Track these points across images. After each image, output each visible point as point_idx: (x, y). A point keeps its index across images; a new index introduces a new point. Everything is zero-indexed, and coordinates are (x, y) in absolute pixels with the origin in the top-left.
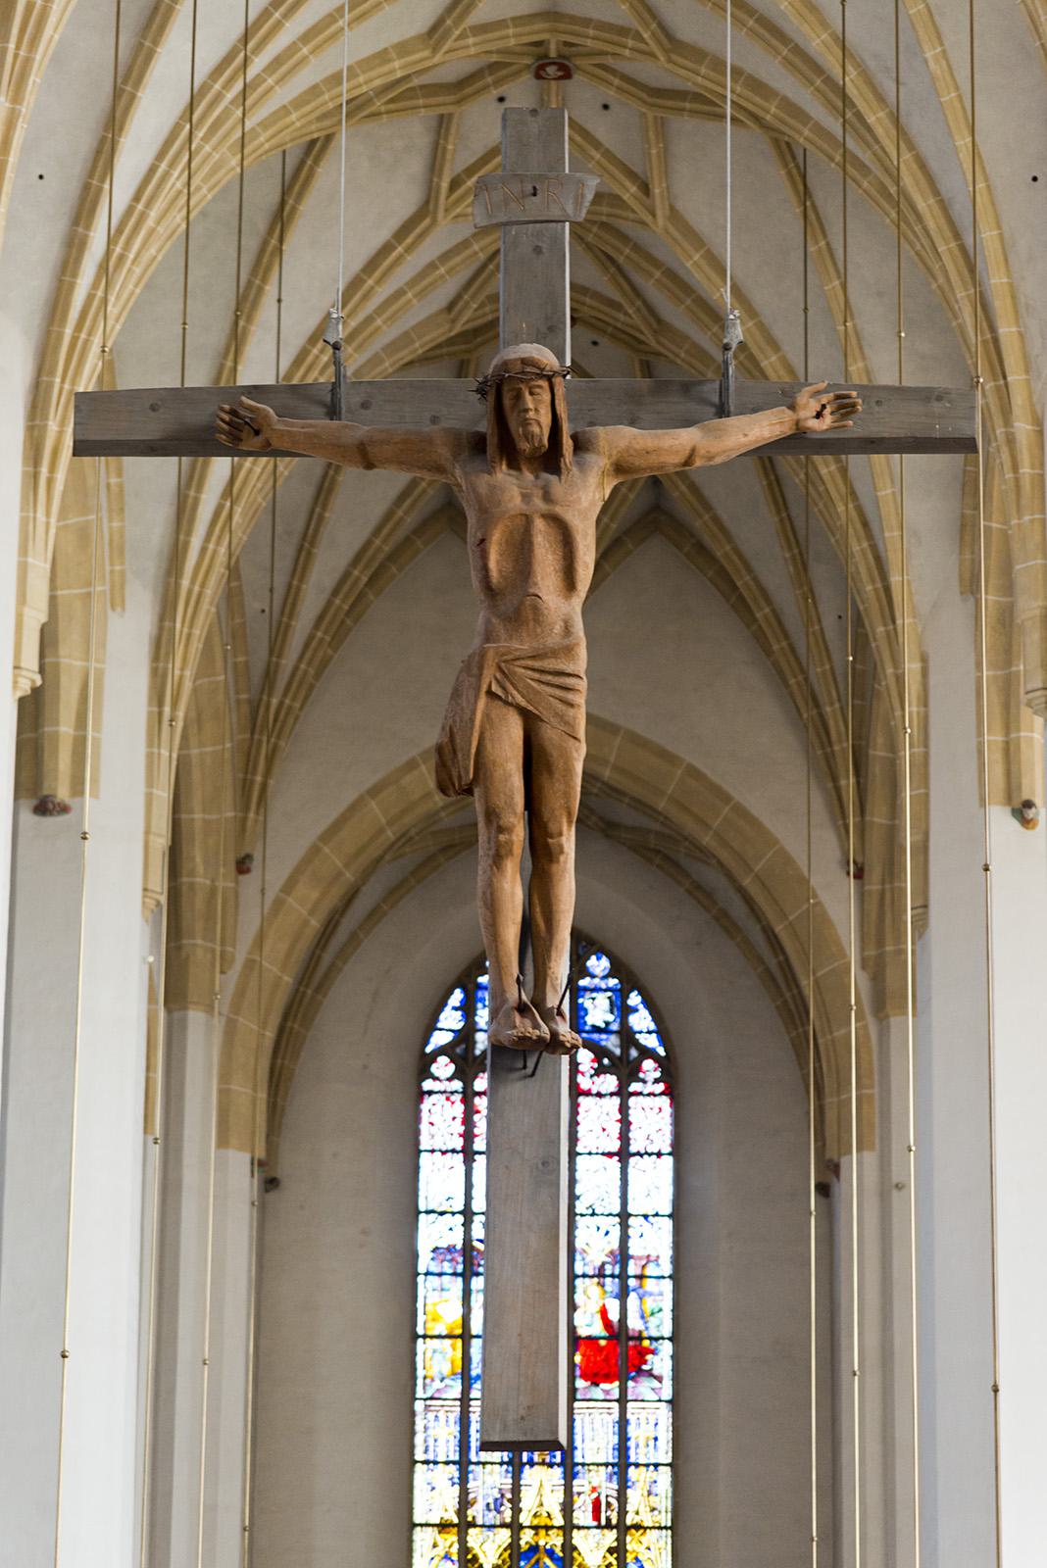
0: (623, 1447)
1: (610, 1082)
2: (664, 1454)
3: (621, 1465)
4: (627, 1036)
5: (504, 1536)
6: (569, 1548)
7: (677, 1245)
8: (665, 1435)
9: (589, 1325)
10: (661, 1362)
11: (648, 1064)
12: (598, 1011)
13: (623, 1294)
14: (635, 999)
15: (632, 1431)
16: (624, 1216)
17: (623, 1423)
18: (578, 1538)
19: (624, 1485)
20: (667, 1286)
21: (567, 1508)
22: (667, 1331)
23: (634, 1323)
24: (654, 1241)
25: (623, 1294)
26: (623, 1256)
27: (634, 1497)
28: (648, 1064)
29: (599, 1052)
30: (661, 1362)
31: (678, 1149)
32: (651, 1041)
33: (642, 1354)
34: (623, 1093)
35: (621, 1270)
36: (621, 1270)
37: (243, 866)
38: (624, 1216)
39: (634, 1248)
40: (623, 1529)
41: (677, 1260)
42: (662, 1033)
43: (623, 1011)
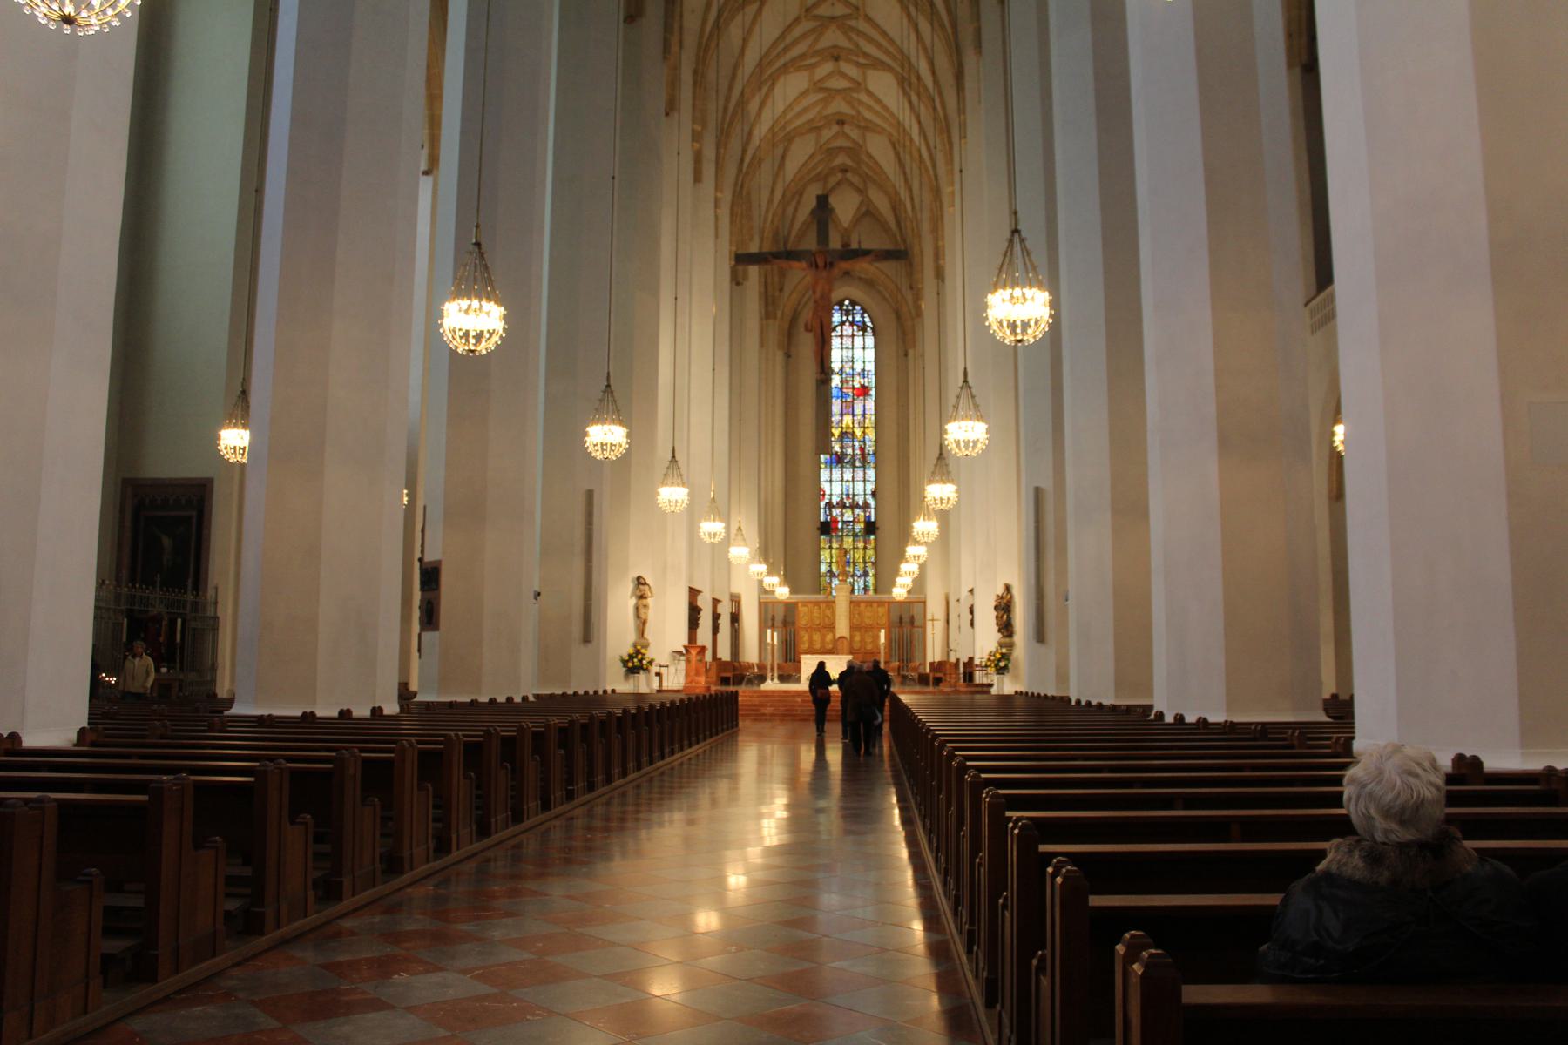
0: (864, 411)
1: (861, 333)
2: (873, 412)
3: (864, 415)
4: (864, 323)
5: (840, 429)
6: (853, 432)
7: (876, 368)
8: (873, 408)
9: (857, 385)
10: (873, 392)
11: (869, 329)
12: (858, 318)
13: (864, 378)
14: (866, 315)
15: (866, 407)
16: (864, 362)
17: (864, 406)
18: (855, 430)
19: (865, 418)
20: (874, 377)
21: (853, 423)
22: (873, 385)
23: (866, 384)
24: (871, 367)
25: (864, 378)
26: (864, 370)
27: (867, 421)
28: (869, 329)
29: (858, 326)
30: (873, 392)
31: (875, 347)
32: (869, 324)
33: (868, 391)
34: (863, 335)
35: (863, 373)
36: (863, 373)
37: (781, 290)
38: (864, 362)
39: (866, 369)
40: (865, 428)
41: (875, 371)
42: (872, 322)
43: (863, 317)
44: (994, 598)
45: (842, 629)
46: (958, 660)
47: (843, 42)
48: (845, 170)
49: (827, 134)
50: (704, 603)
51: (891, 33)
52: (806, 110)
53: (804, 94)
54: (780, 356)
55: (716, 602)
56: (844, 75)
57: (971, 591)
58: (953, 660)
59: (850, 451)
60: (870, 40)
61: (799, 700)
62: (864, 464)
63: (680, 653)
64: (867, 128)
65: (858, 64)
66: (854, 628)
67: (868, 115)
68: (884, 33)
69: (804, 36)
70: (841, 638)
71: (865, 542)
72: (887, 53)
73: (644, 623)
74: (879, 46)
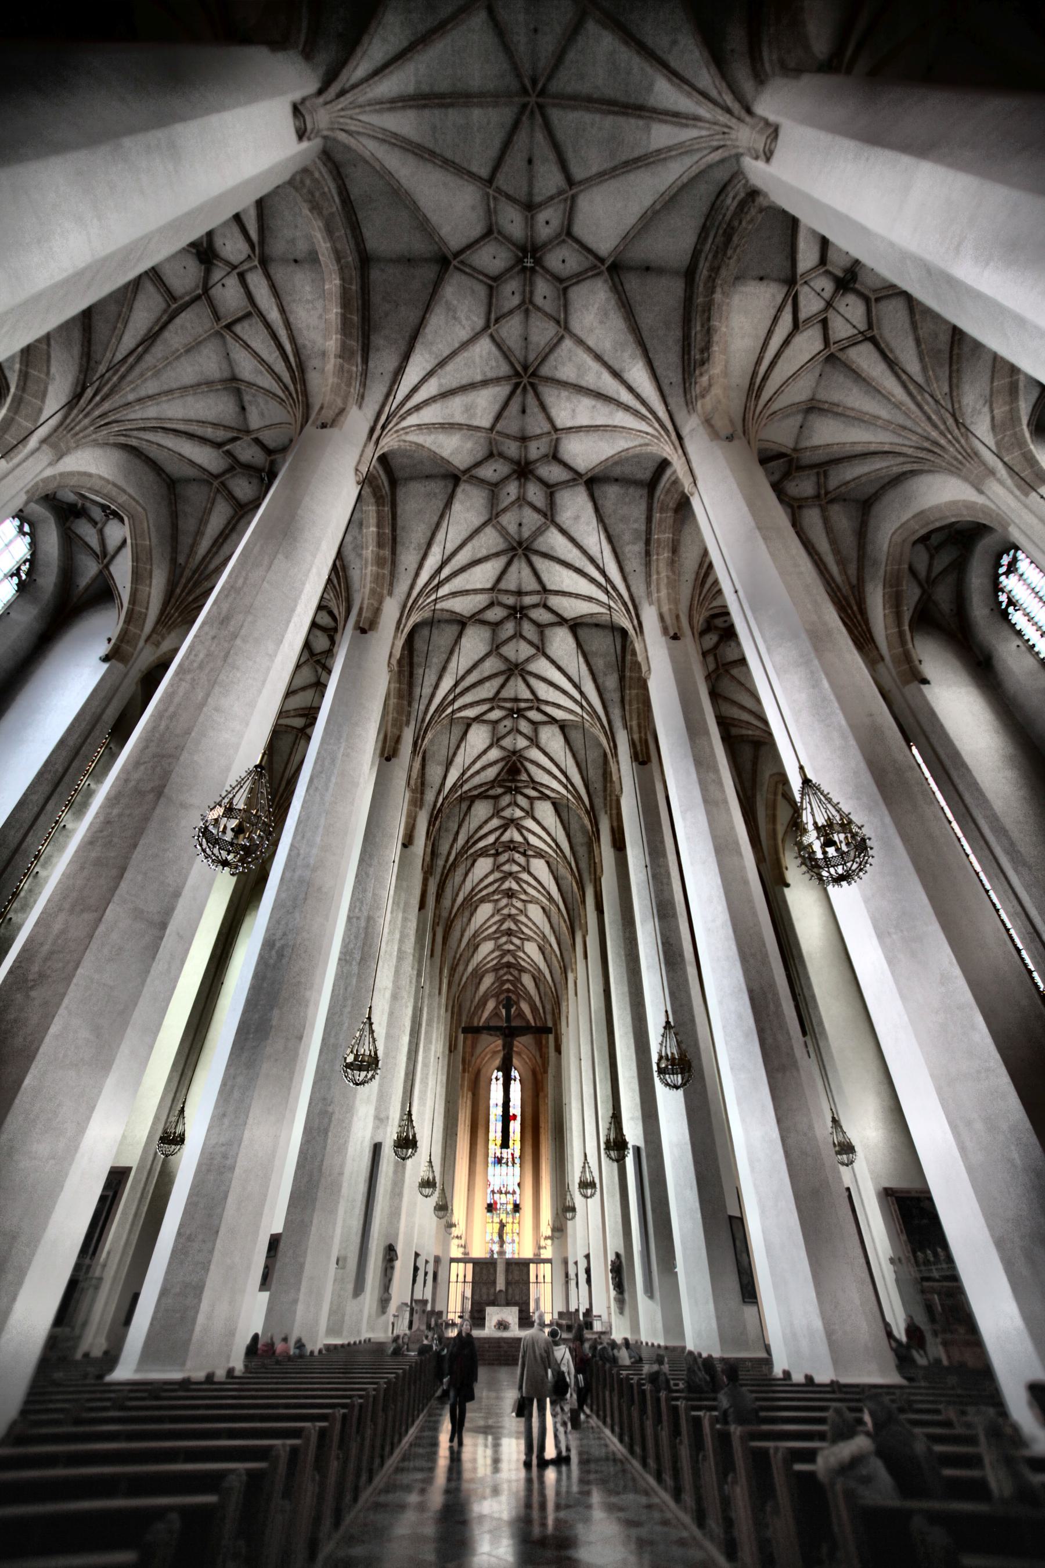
44: (609, 1263)
45: (501, 1284)
46: (577, 1311)
47: (513, 927)
48: (508, 990)
49: (501, 972)
50: (421, 1264)
51: (538, 924)
52: (492, 960)
53: (493, 952)
54: (470, 1095)
55: (427, 1262)
56: (512, 943)
57: (587, 1257)
58: (572, 1309)
59: (505, 1155)
60: (527, 926)
61: (487, 1346)
62: (514, 1163)
63: (406, 1304)
64: (522, 970)
65: (521, 939)
66: (508, 1283)
67: (523, 963)
68: (534, 924)
69: (495, 923)
70: (500, 1291)
71: (513, 1218)
72: (535, 933)
73: (390, 1280)
74: (531, 929)
